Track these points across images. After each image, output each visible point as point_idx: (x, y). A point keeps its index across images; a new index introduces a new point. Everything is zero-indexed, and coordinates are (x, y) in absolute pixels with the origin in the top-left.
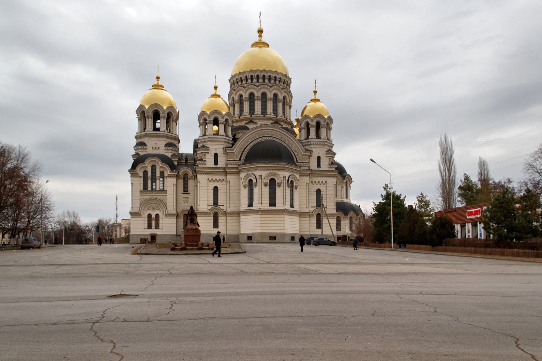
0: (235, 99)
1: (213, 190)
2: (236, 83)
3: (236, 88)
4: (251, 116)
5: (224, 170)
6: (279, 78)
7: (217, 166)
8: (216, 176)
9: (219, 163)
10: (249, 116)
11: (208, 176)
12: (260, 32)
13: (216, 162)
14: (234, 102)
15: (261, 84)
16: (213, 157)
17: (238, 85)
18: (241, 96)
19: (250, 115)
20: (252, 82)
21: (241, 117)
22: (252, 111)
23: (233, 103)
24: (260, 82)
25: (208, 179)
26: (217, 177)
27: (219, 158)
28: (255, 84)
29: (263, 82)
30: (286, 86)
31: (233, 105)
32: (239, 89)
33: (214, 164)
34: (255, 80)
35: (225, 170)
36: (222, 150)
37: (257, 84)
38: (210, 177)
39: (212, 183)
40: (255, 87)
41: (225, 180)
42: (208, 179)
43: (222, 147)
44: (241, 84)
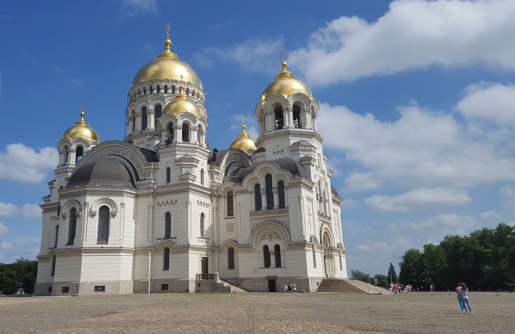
0: (135, 112)
2: (137, 94)
3: (137, 99)
6: (192, 90)
14: (134, 115)
15: (171, 95)
17: (140, 96)
20: (158, 92)
23: (133, 116)
24: (168, 92)
29: (172, 94)
30: (200, 101)
31: (133, 119)
32: (141, 100)
37: (165, 95)
40: (163, 98)
44: (145, 95)
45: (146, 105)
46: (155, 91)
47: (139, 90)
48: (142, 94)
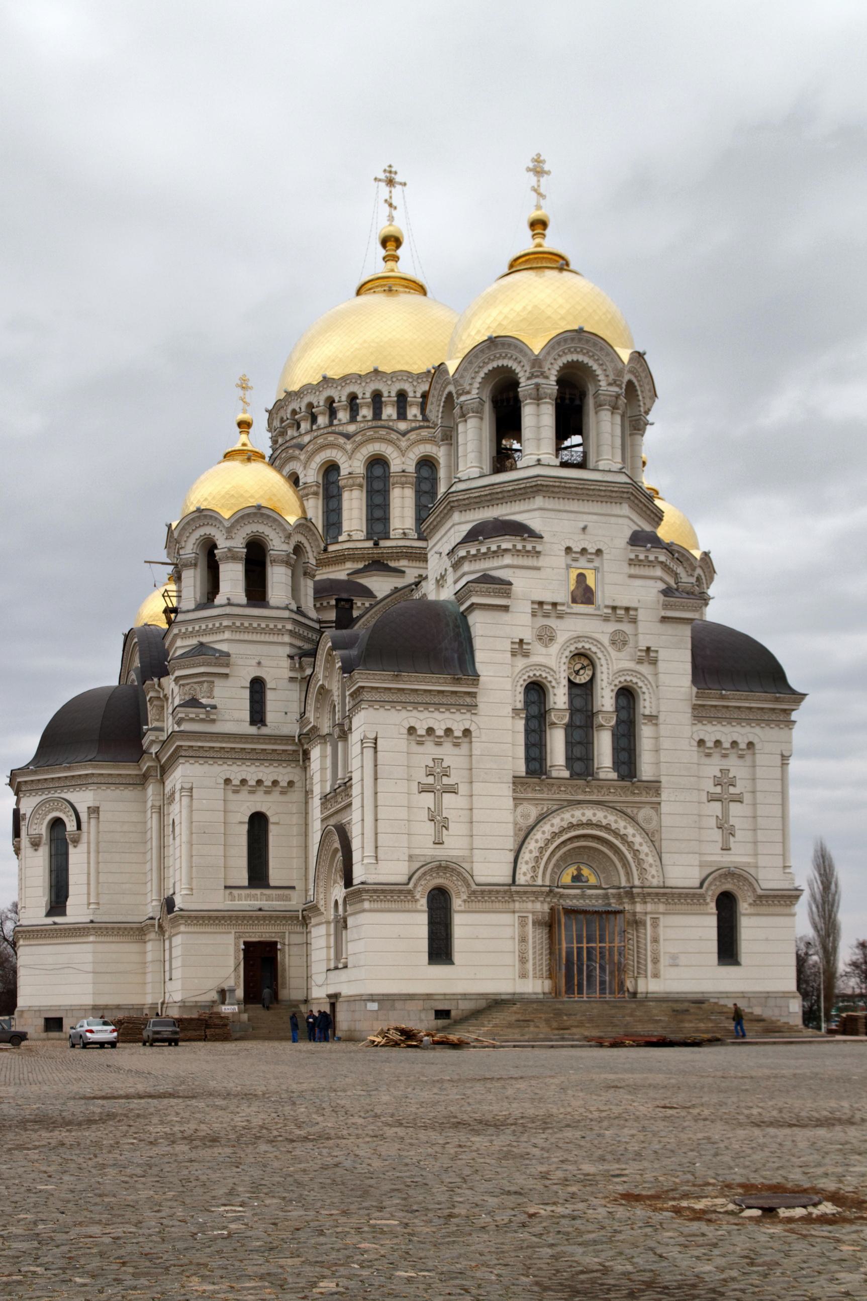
1: (246, 827)
4: (376, 544)
5: (296, 744)
7: (265, 731)
8: (262, 768)
9: (270, 717)
10: (370, 544)
11: (225, 767)
12: (391, 245)
13: (258, 715)
16: (246, 694)
18: (331, 469)
19: (368, 539)
20: (377, 415)
21: (331, 548)
22: (379, 527)
24: (410, 417)
25: (227, 781)
26: (268, 773)
27: (270, 696)
28: (391, 424)
33: (253, 722)
34: (390, 411)
35: (302, 745)
36: (286, 663)
38: (237, 772)
39: (244, 795)
41: (298, 785)
42: (227, 781)
43: (287, 650)
45: (338, 457)
46: (366, 412)
47: (310, 406)
48: (322, 420)
